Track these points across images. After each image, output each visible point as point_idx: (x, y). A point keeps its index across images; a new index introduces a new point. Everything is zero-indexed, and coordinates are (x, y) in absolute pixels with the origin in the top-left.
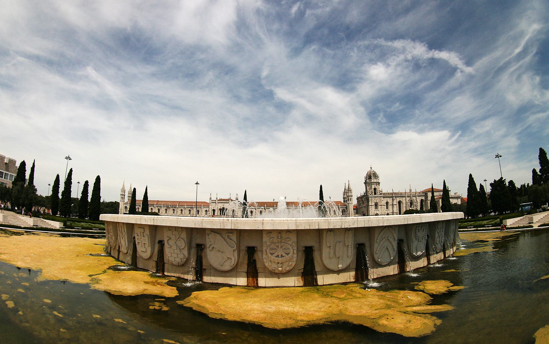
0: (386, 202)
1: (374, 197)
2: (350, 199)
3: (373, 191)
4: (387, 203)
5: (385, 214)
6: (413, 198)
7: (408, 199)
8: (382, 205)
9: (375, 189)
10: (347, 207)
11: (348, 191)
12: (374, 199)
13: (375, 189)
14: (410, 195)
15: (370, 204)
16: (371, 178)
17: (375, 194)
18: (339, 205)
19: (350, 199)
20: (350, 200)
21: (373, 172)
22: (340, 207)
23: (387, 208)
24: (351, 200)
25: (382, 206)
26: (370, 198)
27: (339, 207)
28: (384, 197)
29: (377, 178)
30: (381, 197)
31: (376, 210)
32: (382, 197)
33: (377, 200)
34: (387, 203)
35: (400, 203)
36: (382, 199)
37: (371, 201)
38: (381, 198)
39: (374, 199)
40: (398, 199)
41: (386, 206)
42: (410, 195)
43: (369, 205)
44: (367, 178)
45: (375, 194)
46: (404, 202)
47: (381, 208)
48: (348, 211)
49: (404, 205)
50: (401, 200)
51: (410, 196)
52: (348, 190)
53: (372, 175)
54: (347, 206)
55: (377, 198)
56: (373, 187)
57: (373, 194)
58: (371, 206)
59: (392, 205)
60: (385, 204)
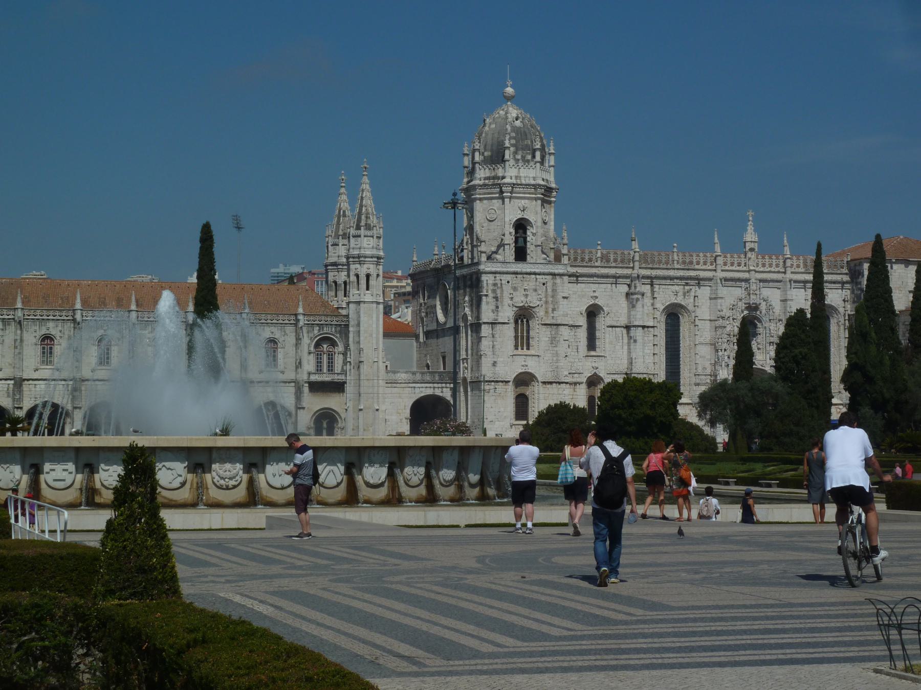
0: (584, 308)
2: (368, 276)
3: (509, 239)
4: (593, 313)
5: (576, 378)
6: (766, 292)
7: (732, 296)
9: (521, 226)
10: (347, 326)
11: (358, 228)
12: (515, 289)
13: (521, 226)
14: (749, 271)
15: (487, 314)
16: (503, 161)
17: (521, 254)
18: (301, 310)
19: (368, 276)
21: (518, 123)
22: (302, 320)
23: (592, 344)
24: (372, 282)
25: (562, 328)
27: (298, 320)
28: (576, 278)
29: (538, 158)
30: (554, 275)
31: (520, 351)
32: (561, 275)
34: (593, 313)
35: (673, 315)
36: (565, 287)
37: (491, 295)
38: (558, 280)
39: (515, 289)
40: (667, 295)
41: (583, 334)
42: (749, 271)
44: (477, 157)
45: (521, 254)
46: (704, 311)
47: (553, 341)
48: (352, 346)
49: (706, 333)
50: (688, 302)
51: (747, 281)
52: (359, 220)
53: (507, 144)
54: (347, 316)
55: (531, 282)
56: (512, 213)
57: (509, 253)
59: (628, 328)
60: (583, 321)
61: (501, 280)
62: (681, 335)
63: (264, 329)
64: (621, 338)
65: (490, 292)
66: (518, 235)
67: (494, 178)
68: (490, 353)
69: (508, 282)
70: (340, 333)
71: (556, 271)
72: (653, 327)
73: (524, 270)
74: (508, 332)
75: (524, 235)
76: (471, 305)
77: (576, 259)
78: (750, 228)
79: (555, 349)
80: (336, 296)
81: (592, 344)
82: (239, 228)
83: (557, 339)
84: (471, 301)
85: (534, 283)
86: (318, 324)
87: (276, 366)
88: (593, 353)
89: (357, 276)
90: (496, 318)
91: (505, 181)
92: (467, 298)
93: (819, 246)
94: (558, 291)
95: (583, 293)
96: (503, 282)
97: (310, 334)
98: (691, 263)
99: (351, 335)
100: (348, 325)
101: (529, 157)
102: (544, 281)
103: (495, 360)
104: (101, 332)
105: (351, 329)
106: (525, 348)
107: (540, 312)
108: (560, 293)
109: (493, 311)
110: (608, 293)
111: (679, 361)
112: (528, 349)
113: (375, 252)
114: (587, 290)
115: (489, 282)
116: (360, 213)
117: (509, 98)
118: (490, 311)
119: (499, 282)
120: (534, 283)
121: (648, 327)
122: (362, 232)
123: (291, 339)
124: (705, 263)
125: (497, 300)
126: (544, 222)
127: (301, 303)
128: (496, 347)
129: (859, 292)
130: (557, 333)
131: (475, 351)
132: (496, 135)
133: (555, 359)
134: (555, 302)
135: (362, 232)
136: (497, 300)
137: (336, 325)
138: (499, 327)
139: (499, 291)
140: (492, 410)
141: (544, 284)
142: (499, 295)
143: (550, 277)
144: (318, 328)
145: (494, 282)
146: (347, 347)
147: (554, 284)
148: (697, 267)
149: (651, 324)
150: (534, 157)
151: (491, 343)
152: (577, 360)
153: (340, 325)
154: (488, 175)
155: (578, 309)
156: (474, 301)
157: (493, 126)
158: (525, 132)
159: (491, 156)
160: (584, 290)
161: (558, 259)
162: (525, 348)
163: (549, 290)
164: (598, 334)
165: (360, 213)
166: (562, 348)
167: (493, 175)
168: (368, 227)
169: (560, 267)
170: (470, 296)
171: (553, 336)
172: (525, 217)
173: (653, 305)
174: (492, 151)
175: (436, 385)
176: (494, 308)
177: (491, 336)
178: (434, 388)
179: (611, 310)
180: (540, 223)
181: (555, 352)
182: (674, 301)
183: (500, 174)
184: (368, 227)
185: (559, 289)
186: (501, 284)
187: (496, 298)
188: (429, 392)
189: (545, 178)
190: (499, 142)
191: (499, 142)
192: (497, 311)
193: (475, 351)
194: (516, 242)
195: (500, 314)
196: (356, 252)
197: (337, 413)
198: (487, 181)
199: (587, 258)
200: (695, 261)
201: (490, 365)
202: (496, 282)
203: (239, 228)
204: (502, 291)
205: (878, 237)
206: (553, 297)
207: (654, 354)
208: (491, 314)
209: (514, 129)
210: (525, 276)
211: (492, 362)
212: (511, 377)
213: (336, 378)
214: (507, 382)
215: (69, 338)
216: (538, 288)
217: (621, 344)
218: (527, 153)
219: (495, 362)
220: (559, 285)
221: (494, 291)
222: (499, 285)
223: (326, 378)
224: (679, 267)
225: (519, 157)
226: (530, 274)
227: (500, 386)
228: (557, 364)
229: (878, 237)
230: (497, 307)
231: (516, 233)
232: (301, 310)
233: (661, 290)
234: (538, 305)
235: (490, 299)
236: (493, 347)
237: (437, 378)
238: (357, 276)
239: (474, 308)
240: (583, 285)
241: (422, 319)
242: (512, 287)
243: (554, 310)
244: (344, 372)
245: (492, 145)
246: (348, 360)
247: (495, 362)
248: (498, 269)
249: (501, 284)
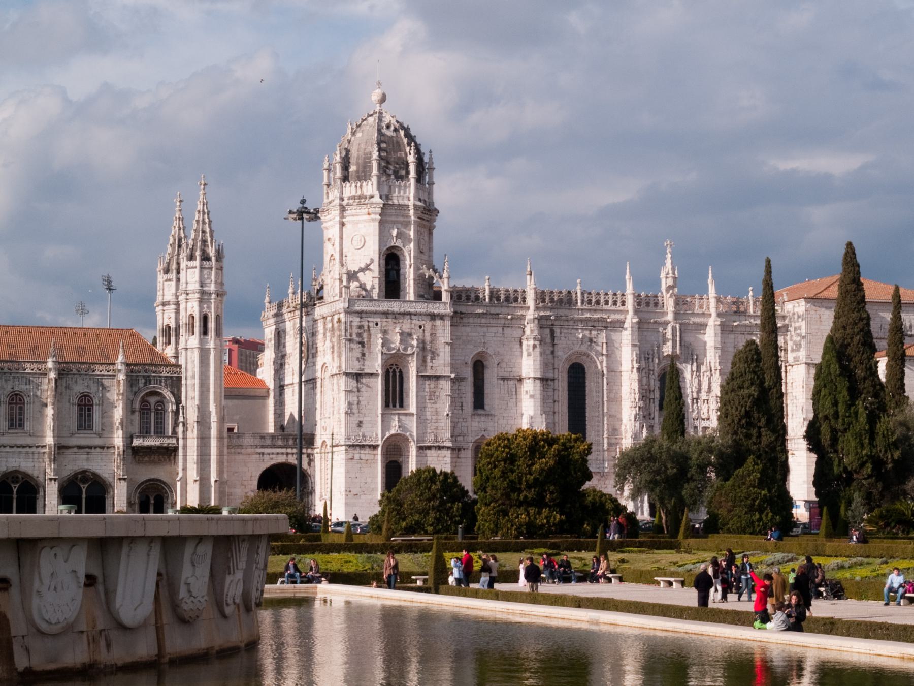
1: (386, 314)
2: (205, 319)
8: (437, 377)
19: (205, 319)
20: (197, 324)
24: (212, 325)
30: (433, 317)
32: (442, 317)
38: (438, 323)
39: (385, 332)
41: (468, 389)
43: (340, 367)
60: (468, 373)
61: (368, 321)
62: (587, 389)
63: (76, 382)
64: (514, 393)
65: (354, 337)
66: (390, 267)
67: (360, 197)
69: (377, 324)
70: (172, 386)
71: (436, 311)
72: (553, 380)
73: (396, 310)
74: (378, 384)
75: (396, 268)
76: (333, 352)
77: (459, 297)
78: (668, 262)
79: (434, 406)
80: (169, 343)
81: (479, 402)
82: (110, 289)
83: (437, 394)
84: (333, 348)
85: (408, 326)
86: (144, 376)
87: (90, 428)
88: (480, 411)
90: (362, 367)
91: (373, 200)
92: (328, 344)
93: (768, 262)
94: (438, 335)
95: (468, 338)
96: (371, 324)
97: (134, 388)
98: (598, 302)
99: (183, 389)
100: (179, 378)
101: (403, 172)
102: (422, 323)
103: (360, 419)
105: (183, 382)
106: (397, 405)
108: (440, 339)
109: (358, 359)
110: (499, 339)
111: (585, 421)
112: (401, 406)
114: (474, 334)
115: (353, 324)
118: (355, 359)
119: (365, 324)
120: (408, 326)
121: (547, 380)
124: (615, 303)
125: (363, 346)
126: (421, 252)
127: (121, 350)
128: (362, 403)
129: (799, 338)
130: (436, 387)
131: (336, 408)
132: (363, 146)
133: (434, 418)
136: (363, 346)
137: (166, 377)
138: (364, 380)
139: (365, 335)
140: (357, 480)
141: (420, 327)
142: (365, 340)
143: (428, 319)
144: (143, 381)
145: (359, 324)
146: (178, 401)
147: (434, 326)
148: (605, 307)
149: (550, 375)
150: (408, 173)
151: (356, 399)
152: (461, 420)
153: (171, 377)
154: (353, 193)
155: (463, 358)
156: (336, 348)
157: (359, 135)
158: (398, 142)
159: (357, 172)
160: (470, 334)
162: (397, 405)
163: (427, 334)
164: (487, 390)
167: (359, 192)
169: (442, 306)
170: (331, 341)
171: (432, 390)
172: (396, 244)
173: (553, 352)
174: (358, 164)
175: (289, 450)
176: (359, 355)
177: (355, 390)
178: (287, 454)
179: (502, 360)
181: (433, 410)
182: (576, 348)
185: (440, 332)
186: (369, 327)
187: (362, 344)
188: (282, 459)
189: (422, 198)
190: (365, 154)
191: (365, 154)
192: (364, 359)
193: (336, 408)
195: (366, 363)
197: (164, 483)
198: (351, 201)
199: (473, 295)
200: (602, 300)
201: (354, 426)
202: (363, 323)
204: (370, 335)
205: (850, 245)
206: (431, 342)
207: (554, 413)
208: (356, 363)
210: (397, 316)
211: (357, 422)
212: (380, 442)
213: (166, 442)
214: (375, 447)
216: (413, 331)
217: (514, 400)
218: (401, 168)
219: (361, 422)
220: (439, 328)
221: (359, 335)
222: (366, 328)
223: (152, 442)
224: (584, 307)
225: (391, 172)
226: (404, 314)
227: (366, 454)
228: (436, 424)
229: (850, 245)
230: (363, 355)
231: (387, 263)
232: (121, 358)
233: (563, 335)
234: (414, 353)
236: (358, 404)
237: (291, 442)
239: (336, 355)
240: (468, 329)
242: (381, 330)
243: (432, 359)
244: (175, 432)
245: (358, 158)
246: (181, 419)
247: (361, 422)
248: (364, 309)
249: (369, 327)
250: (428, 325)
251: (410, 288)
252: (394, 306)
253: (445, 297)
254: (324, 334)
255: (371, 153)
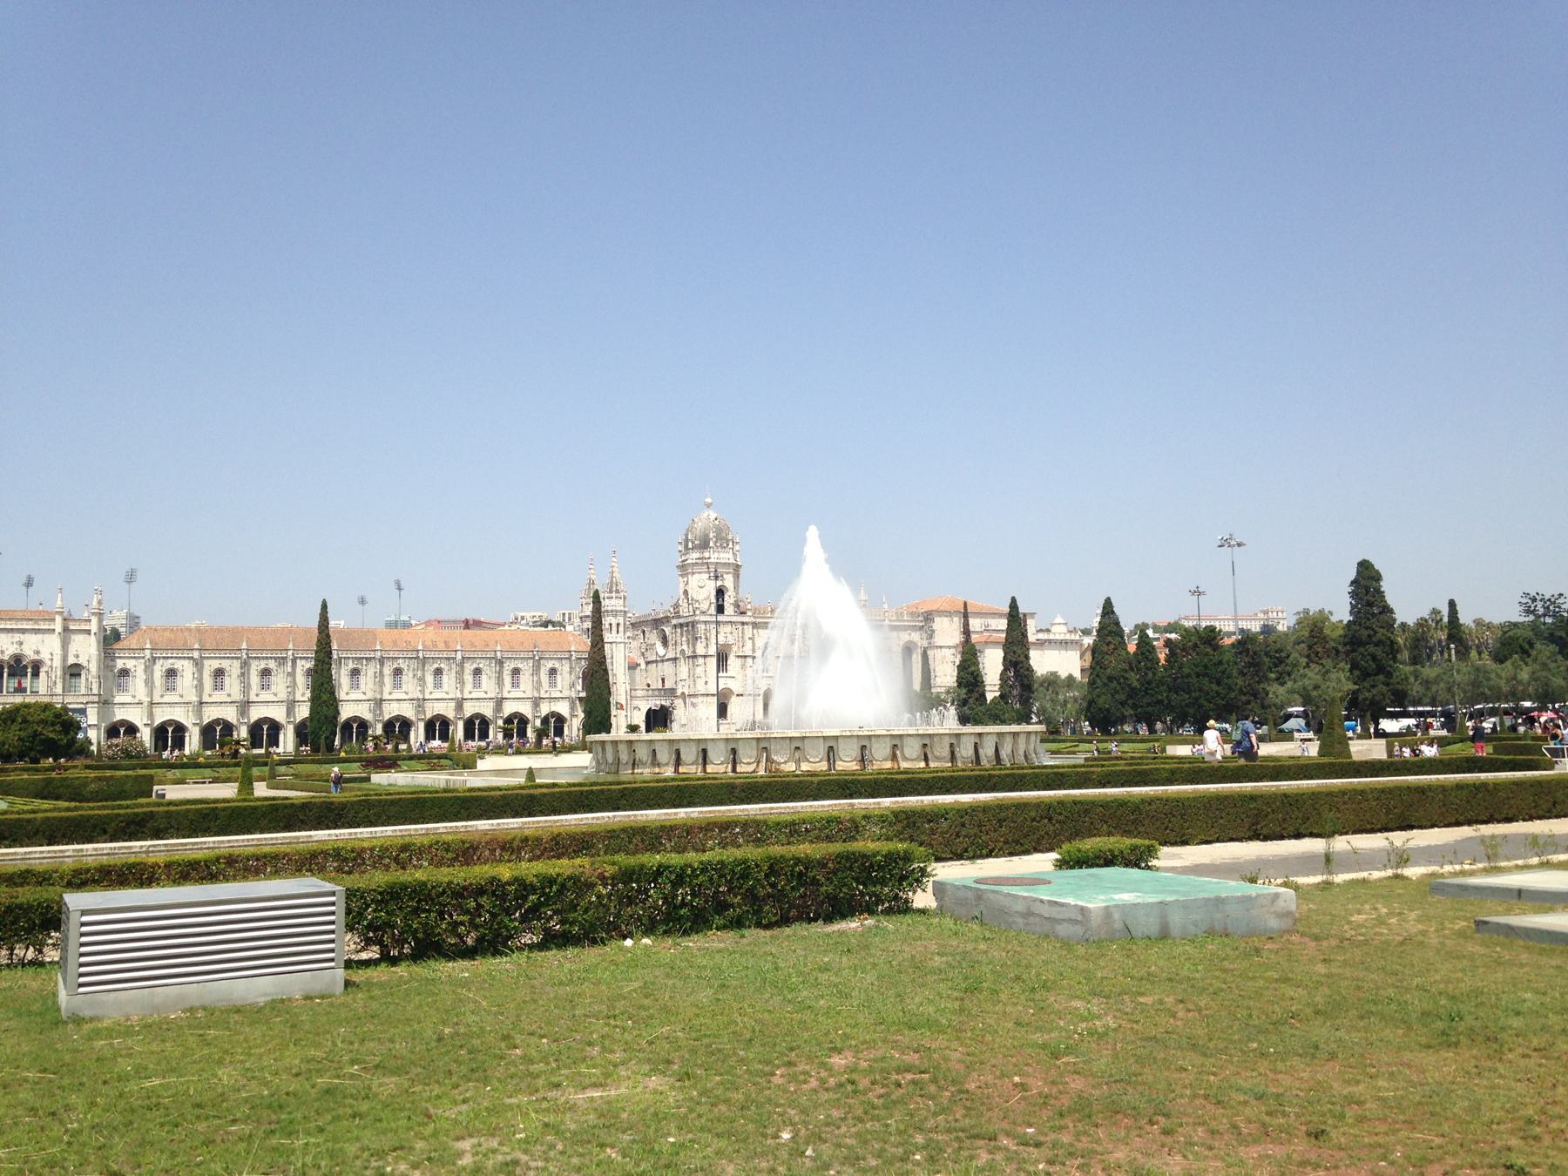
2: (618, 624)
5: (757, 692)
8: (746, 657)
11: (611, 592)
17: (720, 609)
22: (574, 655)
26: (703, 626)
29: (731, 546)
30: (743, 623)
32: (747, 623)
33: (727, 635)
38: (746, 627)
43: (694, 652)
44: (690, 545)
45: (720, 609)
47: (743, 666)
52: (611, 587)
53: (711, 535)
57: (713, 610)
58: (705, 656)
67: (702, 558)
68: (703, 675)
74: (714, 661)
82: (400, 589)
89: (611, 624)
92: (684, 639)
104: (436, 666)
107: (735, 648)
113: (622, 608)
116: (612, 581)
117: (709, 506)
122: (614, 595)
123: (566, 668)
134: (743, 641)
135: (614, 595)
138: (708, 659)
161: (743, 613)
165: (612, 581)
166: (749, 672)
168: (617, 591)
180: (732, 588)
183: (707, 555)
184: (617, 591)
187: (707, 639)
194: (718, 601)
196: (610, 608)
203: (400, 589)
209: (715, 526)
215: (414, 670)
221: (705, 634)
226: (727, 622)
229: (1014, 600)
235: (703, 640)
238: (611, 624)
241: (643, 654)
250: (740, 627)
251: (729, 609)
252: (720, 618)
253: (749, 613)
254: (682, 635)
255: (707, 535)
